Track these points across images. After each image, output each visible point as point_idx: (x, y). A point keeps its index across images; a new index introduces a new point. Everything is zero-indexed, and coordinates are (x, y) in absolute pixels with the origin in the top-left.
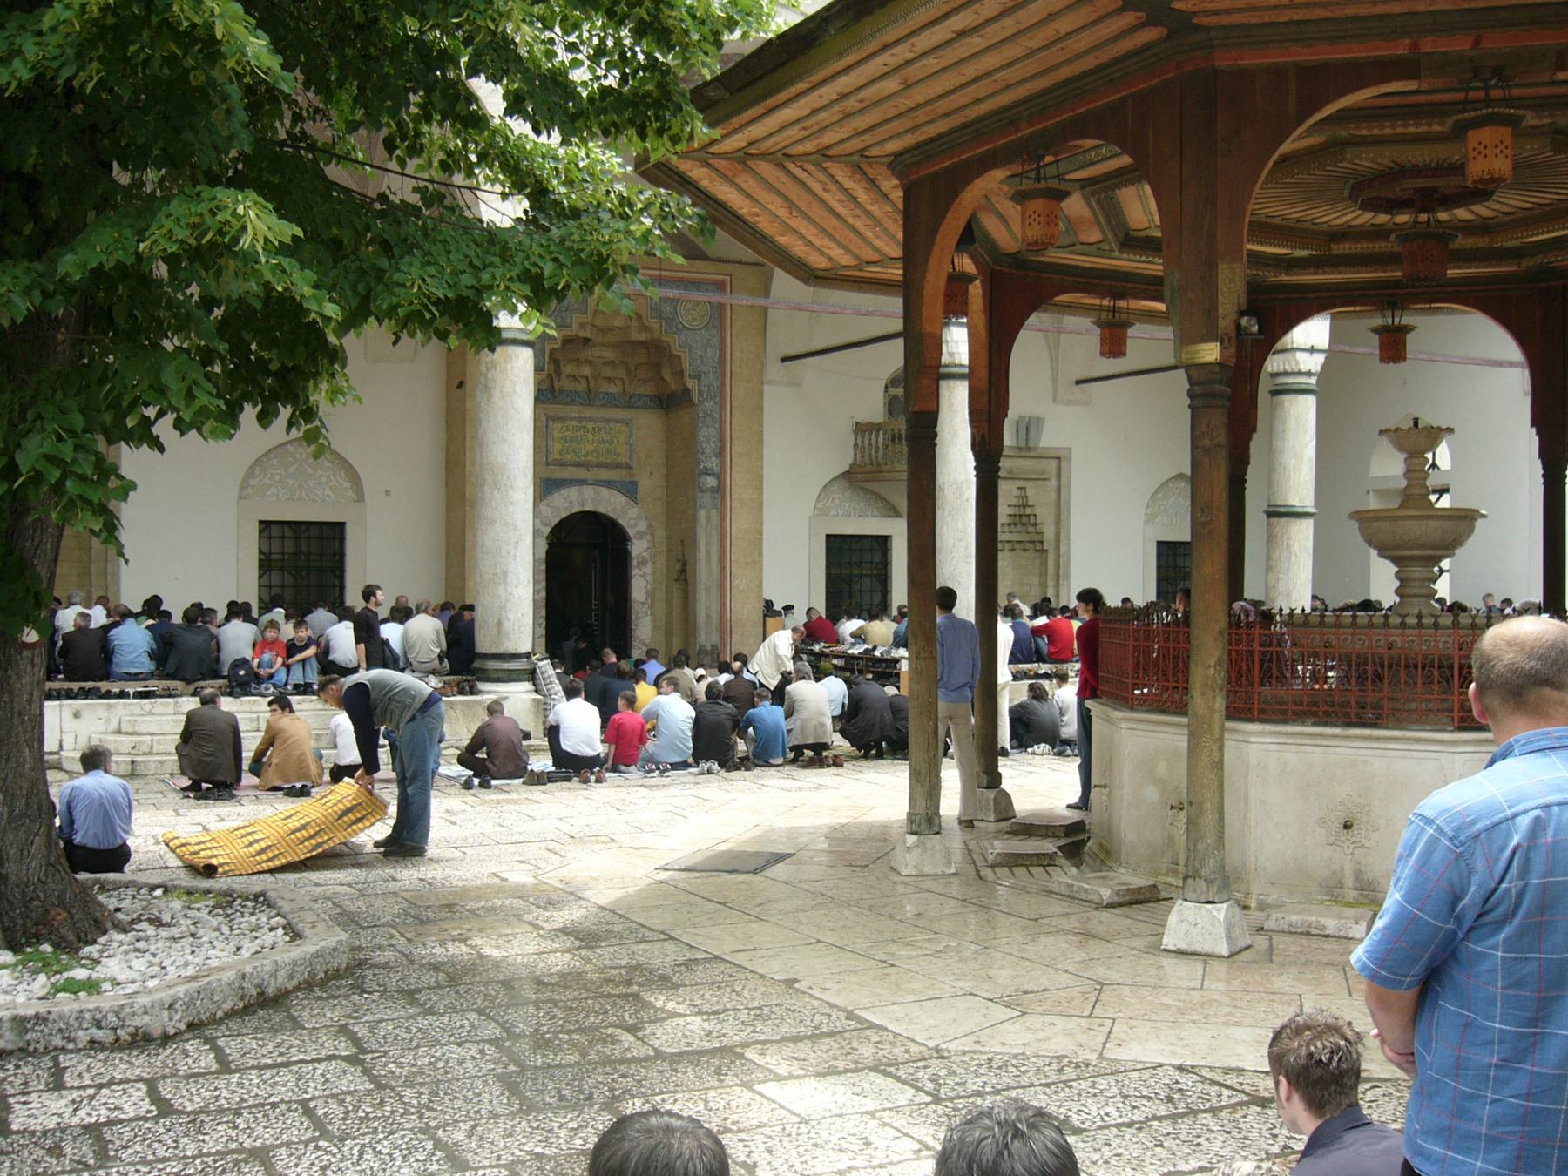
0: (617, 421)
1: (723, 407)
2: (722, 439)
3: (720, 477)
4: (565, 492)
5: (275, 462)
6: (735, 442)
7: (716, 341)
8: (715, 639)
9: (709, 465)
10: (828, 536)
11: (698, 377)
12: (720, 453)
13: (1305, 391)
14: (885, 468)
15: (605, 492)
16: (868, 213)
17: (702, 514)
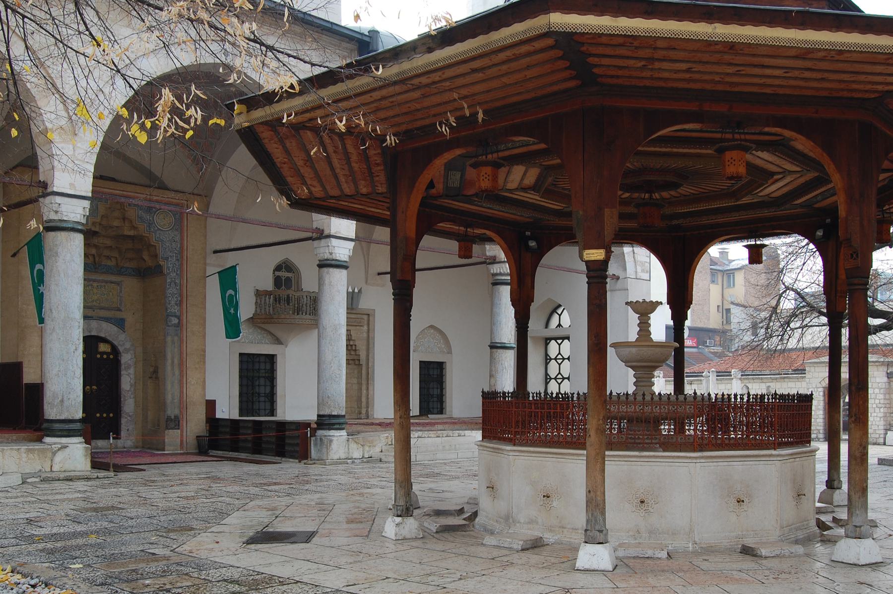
1: (181, 277)
2: (181, 295)
3: (179, 318)
10: (241, 354)
11: (167, 259)
12: (180, 304)
13: (506, 284)
14: (275, 317)
15: (104, 325)
16: (351, 168)
17: (169, 339)
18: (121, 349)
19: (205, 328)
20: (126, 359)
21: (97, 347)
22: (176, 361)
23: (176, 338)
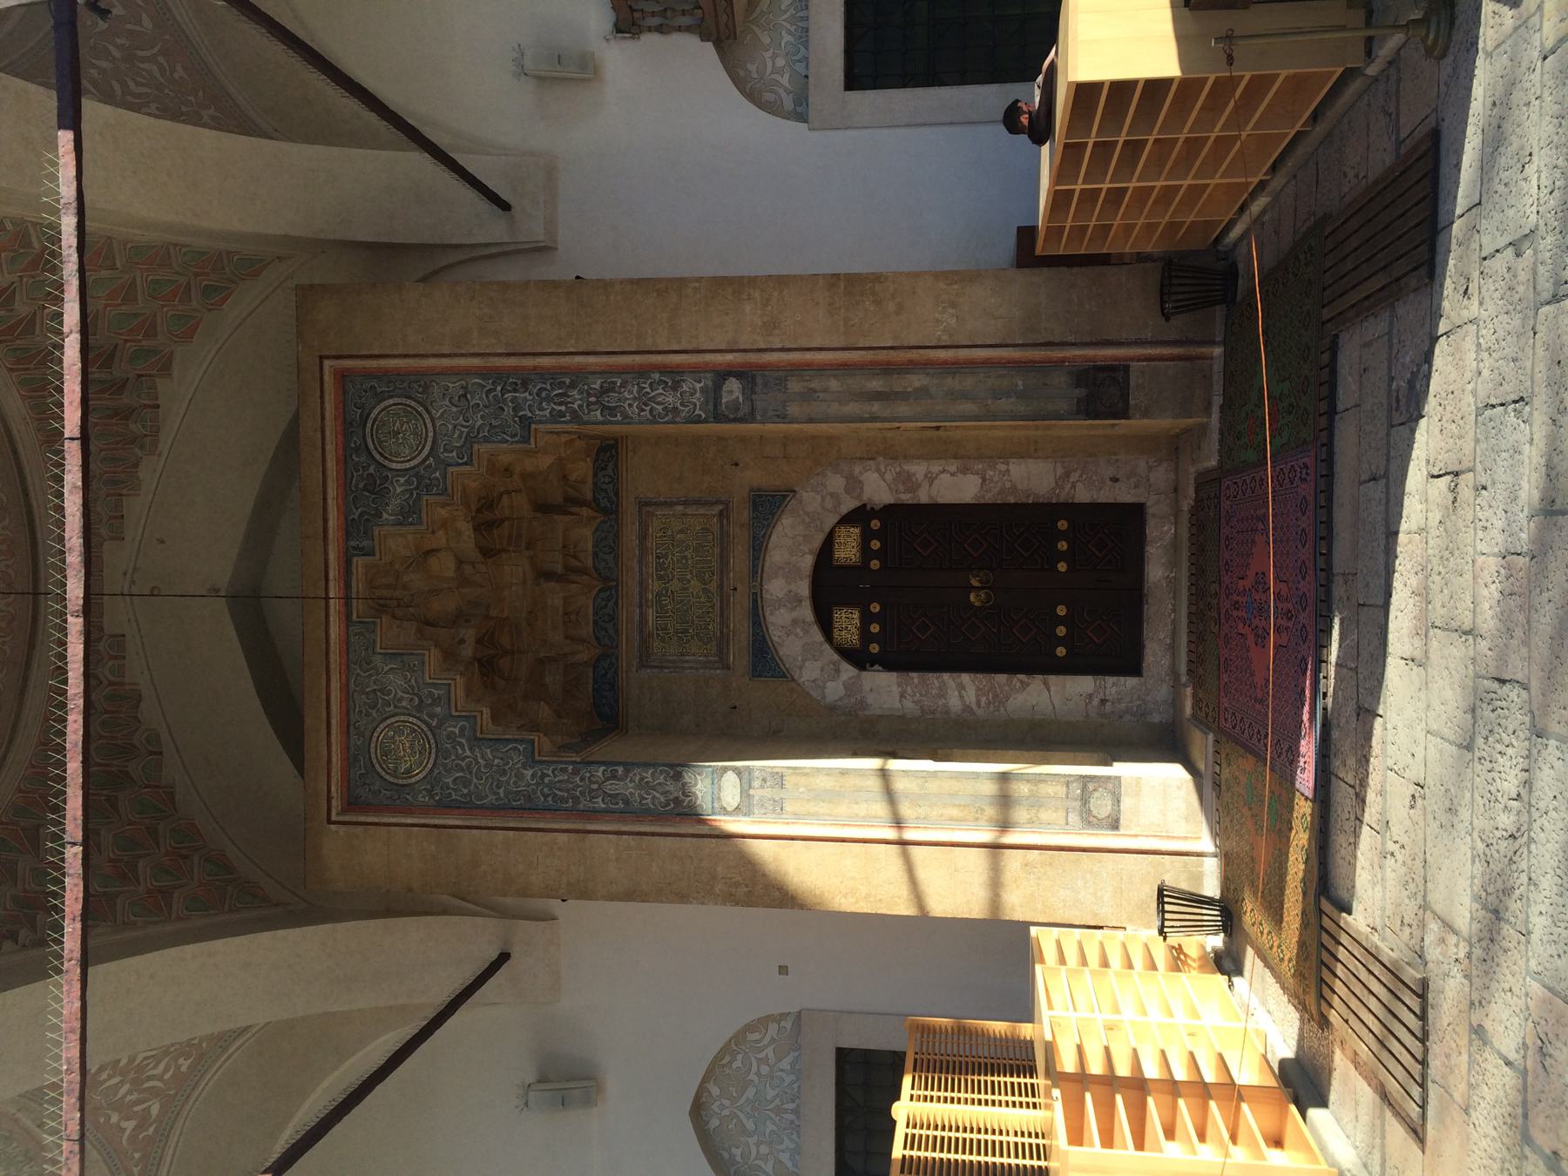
0: (643, 537)
2: (642, 372)
3: (722, 374)
4: (775, 634)
5: (737, 1152)
6: (648, 344)
7: (454, 386)
8: (1060, 380)
9: (698, 398)
10: (854, 80)
12: (674, 376)
18: (849, 505)
19: (752, 281)
20: (878, 488)
21: (847, 569)
22: (876, 384)
23: (795, 386)
